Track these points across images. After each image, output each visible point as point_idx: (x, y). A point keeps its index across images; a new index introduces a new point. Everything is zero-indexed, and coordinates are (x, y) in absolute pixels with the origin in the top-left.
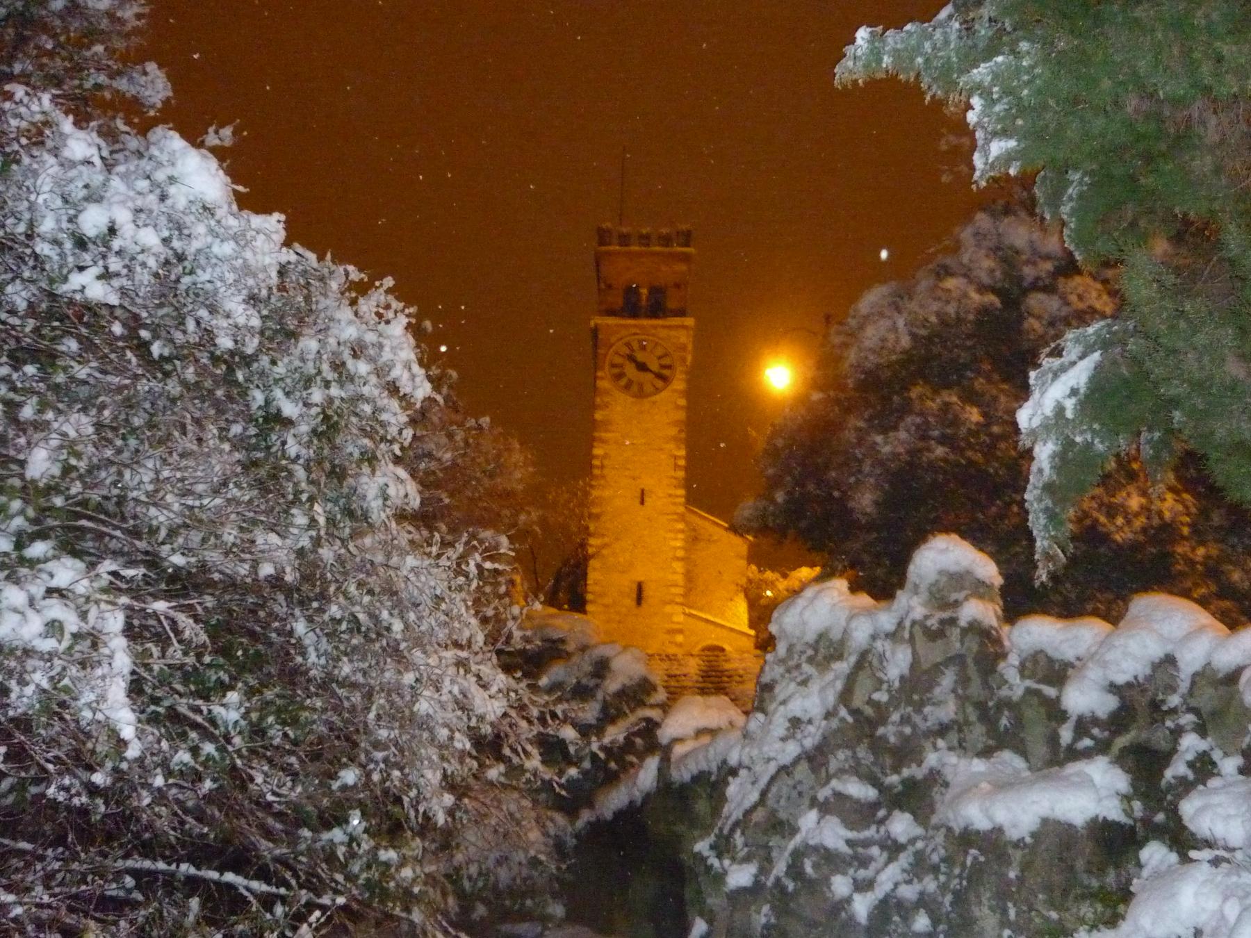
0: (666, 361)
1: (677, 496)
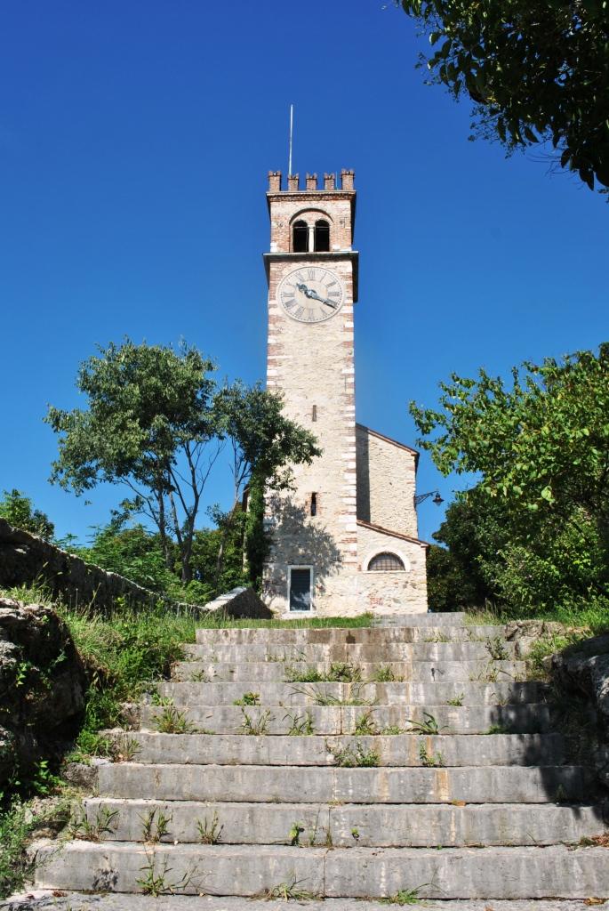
0: (335, 289)
1: (348, 412)
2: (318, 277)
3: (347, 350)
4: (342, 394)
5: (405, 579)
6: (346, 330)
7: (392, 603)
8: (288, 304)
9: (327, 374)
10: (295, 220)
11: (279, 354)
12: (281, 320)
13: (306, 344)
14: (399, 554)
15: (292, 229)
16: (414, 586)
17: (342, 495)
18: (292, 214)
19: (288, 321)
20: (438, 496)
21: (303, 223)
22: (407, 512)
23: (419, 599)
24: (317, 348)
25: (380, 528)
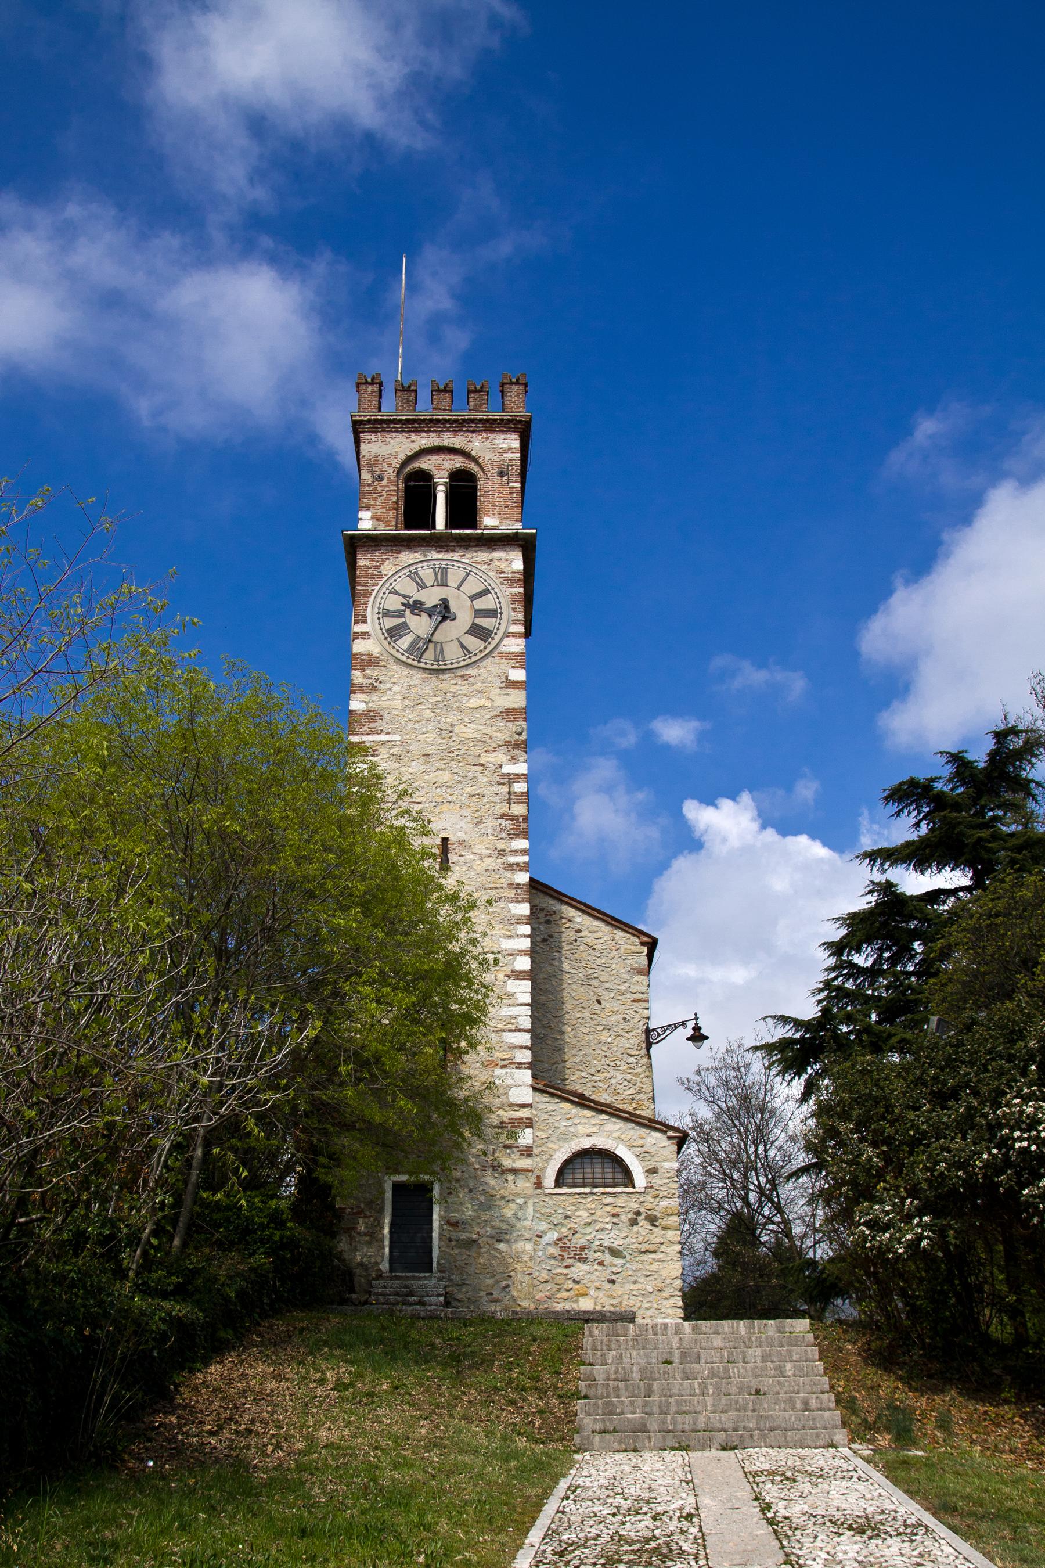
0: (487, 602)
1: (515, 852)
2: (453, 579)
3: (514, 727)
4: (503, 816)
5: (635, 1206)
6: (512, 685)
7: (608, 1258)
8: (394, 633)
9: (471, 774)
10: (408, 469)
11: (372, 732)
12: (377, 664)
13: (427, 713)
14: (622, 1152)
15: (402, 486)
16: (652, 1220)
17: (500, 1026)
18: (402, 457)
19: (394, 667)
20: (697, 1028)
21: (425, 476)
22: (632, 1060)
23: (663, 1248)
24: (448, 720)
25: (582, 1096)
